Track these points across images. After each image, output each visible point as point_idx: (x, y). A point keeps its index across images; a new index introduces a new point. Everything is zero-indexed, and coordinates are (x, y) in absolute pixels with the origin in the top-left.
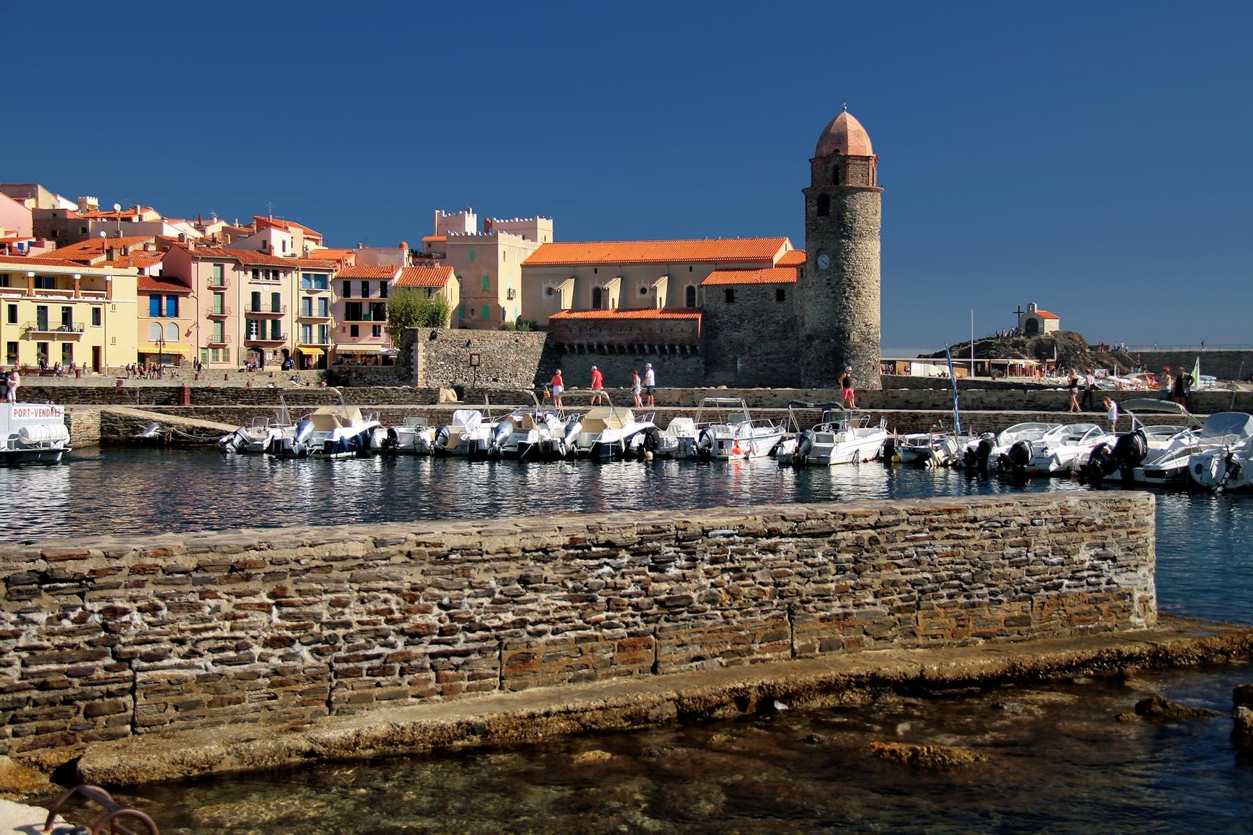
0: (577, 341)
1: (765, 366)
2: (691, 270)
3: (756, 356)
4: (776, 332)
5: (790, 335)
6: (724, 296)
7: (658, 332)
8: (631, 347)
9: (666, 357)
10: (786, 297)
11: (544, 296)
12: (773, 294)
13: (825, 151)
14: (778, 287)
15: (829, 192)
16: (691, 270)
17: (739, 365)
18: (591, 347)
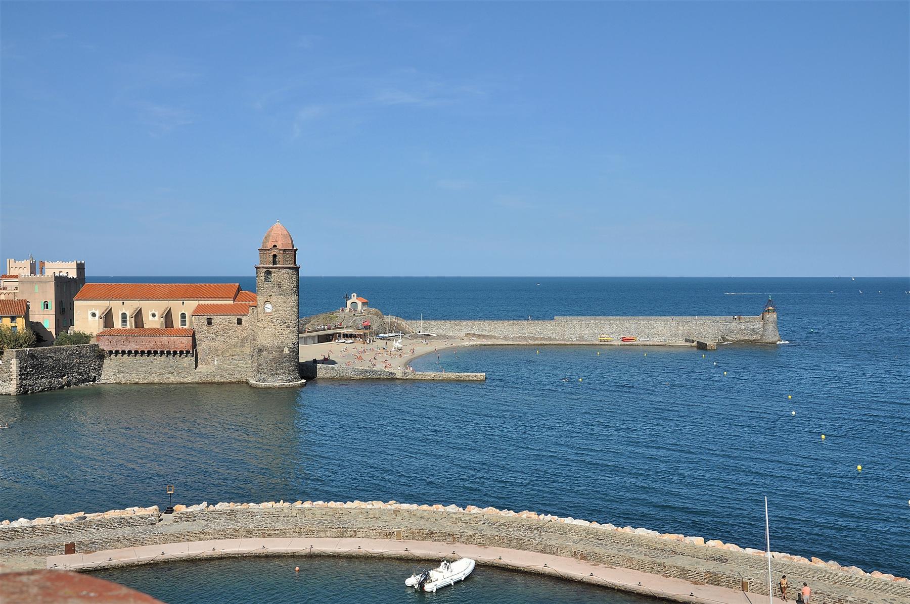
3: (226, 357)
4: (237, 343)
11: (90, 316)
13: (269, 245)
14: (239, 317)
17: (216, 362)
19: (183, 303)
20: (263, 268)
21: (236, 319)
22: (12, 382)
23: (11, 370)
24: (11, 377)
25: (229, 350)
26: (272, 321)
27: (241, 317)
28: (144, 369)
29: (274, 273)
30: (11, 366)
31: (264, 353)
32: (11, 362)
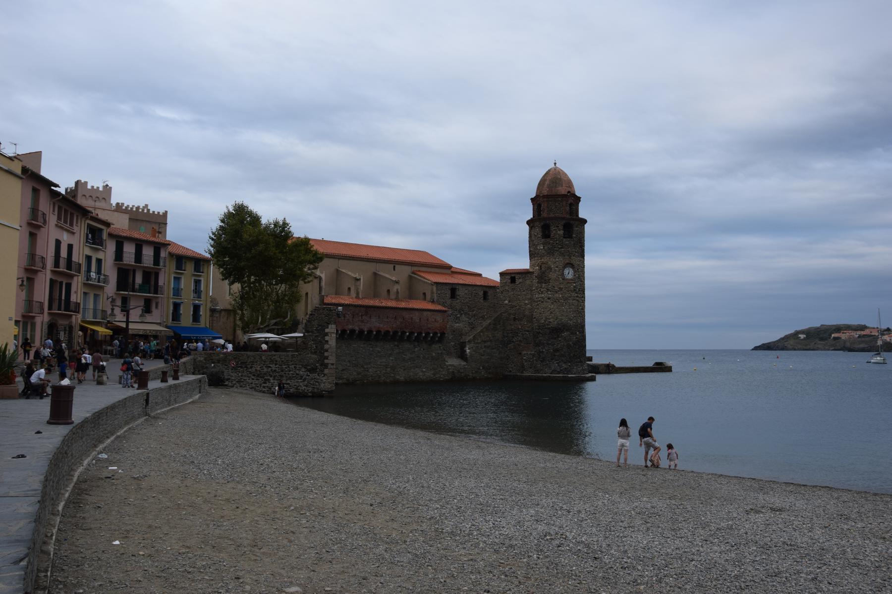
0: (350, 327)
1: (484, 351)
2: (394, 269)
3: (478, 343)
4: (490, 324)
5: (498, 327)
6: (449, 292)
7: (418, 321)
8: (395, 333)
9: (416, 344)
10: (490, 298)
12: (481, 293)
14: (485, 289)
15: (571, 222)
16: (394, 269)
18: (361, 332)
19: (394, 266)
20: (563, 219)
21: (482, 292)
22: (326, 371)
23: (326, 347)
24: (326, 361)
25: (482, 334)
26: (575, 290)
27: (487, 290)
28: (384, 360)
29: (577, 227)
30: (327, 338)
31: (566, 334)
32: (327, 330)
